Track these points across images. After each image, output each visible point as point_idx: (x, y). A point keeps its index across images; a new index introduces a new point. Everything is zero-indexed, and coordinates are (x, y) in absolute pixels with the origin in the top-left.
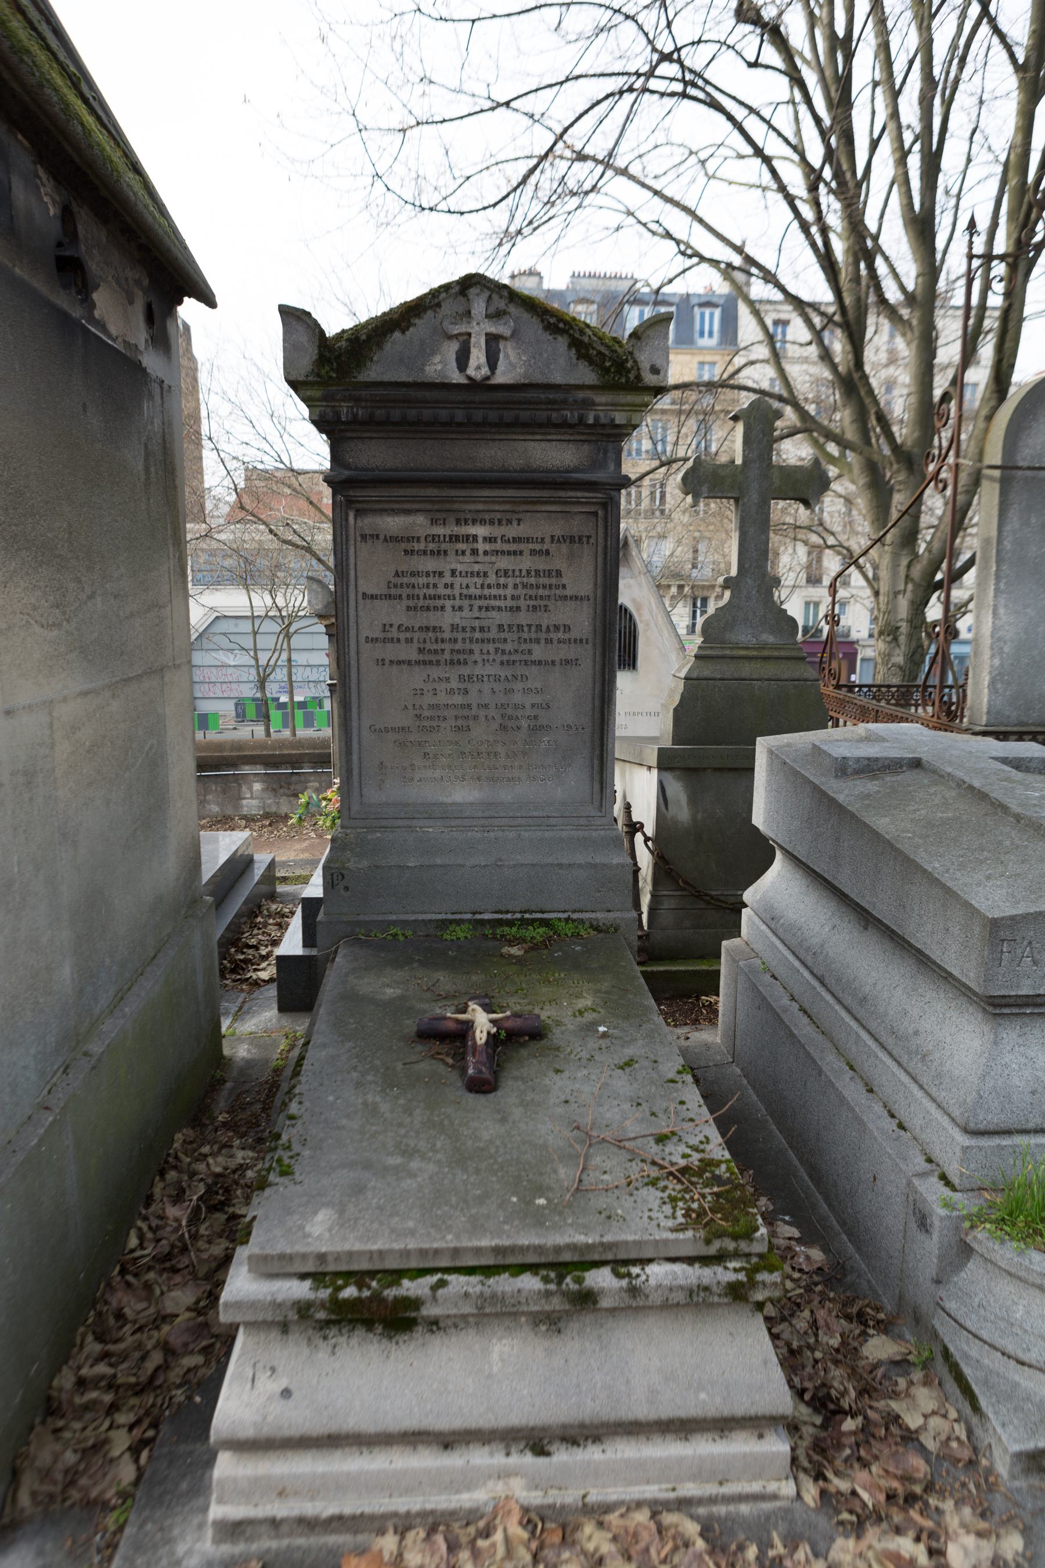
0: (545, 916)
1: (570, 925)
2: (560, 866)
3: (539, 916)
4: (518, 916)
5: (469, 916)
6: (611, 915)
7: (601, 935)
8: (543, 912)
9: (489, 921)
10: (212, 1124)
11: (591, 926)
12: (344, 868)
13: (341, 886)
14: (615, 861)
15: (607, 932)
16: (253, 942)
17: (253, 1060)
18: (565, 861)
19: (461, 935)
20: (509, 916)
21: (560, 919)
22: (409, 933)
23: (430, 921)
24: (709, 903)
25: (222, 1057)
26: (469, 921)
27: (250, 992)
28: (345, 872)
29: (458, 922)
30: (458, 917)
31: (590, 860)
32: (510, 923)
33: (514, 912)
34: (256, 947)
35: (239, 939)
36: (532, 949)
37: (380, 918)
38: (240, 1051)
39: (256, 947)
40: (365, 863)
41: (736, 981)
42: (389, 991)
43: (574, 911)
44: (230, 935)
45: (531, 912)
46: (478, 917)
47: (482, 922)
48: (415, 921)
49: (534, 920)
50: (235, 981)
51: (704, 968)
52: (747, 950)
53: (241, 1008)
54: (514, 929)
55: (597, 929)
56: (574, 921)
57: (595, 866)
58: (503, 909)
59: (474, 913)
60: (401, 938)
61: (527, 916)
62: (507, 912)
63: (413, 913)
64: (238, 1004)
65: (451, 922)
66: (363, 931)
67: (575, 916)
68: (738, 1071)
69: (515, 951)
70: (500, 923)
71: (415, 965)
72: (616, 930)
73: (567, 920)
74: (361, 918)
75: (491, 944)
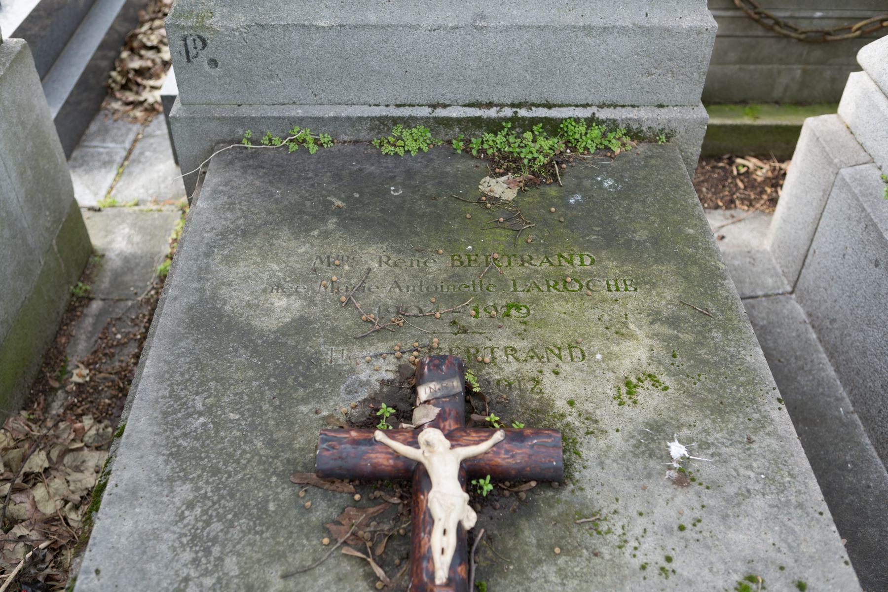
0: (554, 113)
1: (595, 132)
2: (588, 30)
3: (542, 113)
4: (508, 112)
5: (425, 112)
6: (664, 115)
7: (642, 148)
8: (549, 106)
9: (459, 121)
10: (63, 387)
11: (629, 133)
12: (203, 27)
13: (203, 58)
14: (685, 24)
15: (653, 140)
16: (154, 40)
17: (134, 256)
18: (597, 22)
19: (412, 145)
20: (492, 113)
21: (577, 120)
22: (325, 138)
23: (360, 119)
24: (770, 28)
25: (91, 251)
26: (426, 121)
27: (146, 123)
28: (206, 35)
29: (408, 122)
30: (406, 112)
31: (641, 20)
32: (494, 126)
33: (501, 106)
34: (156, 49)
35: (135, 36)
36: (530, 184)
37: (275, 112)
38: (114, 240)
39: (156, 49)
40: (241, 19)
41: (827, 195)
42: (279, 302)
43: (601, 106)
44: (122, 29)
45: (529, 105)
46: (441, 113)
47: (447, 122)
48: (336, 119)
49: (534, 121)
50: (128, 104)
51: (747, 121)
52: (852, 144)
53: (130, 152)
54: (500, 138)
55: (635, 135)
56: (600, 122)
57: (647, 31)
58: (485, 100)
59: (434, 106)
60: (313, 149)
61: (523, 113)
62: (490, 105)
63: (331, 103)
64: (127, 145)
65: (395, 121)
66: (249, 134)
67: (603, 114)
68: (800, 311)
69: (501, 188)
70: (477, 122)
71: (332, 223)
72: (668, 138)
73: (591, 121)
74: (245, 111)
75: (463, 165)
